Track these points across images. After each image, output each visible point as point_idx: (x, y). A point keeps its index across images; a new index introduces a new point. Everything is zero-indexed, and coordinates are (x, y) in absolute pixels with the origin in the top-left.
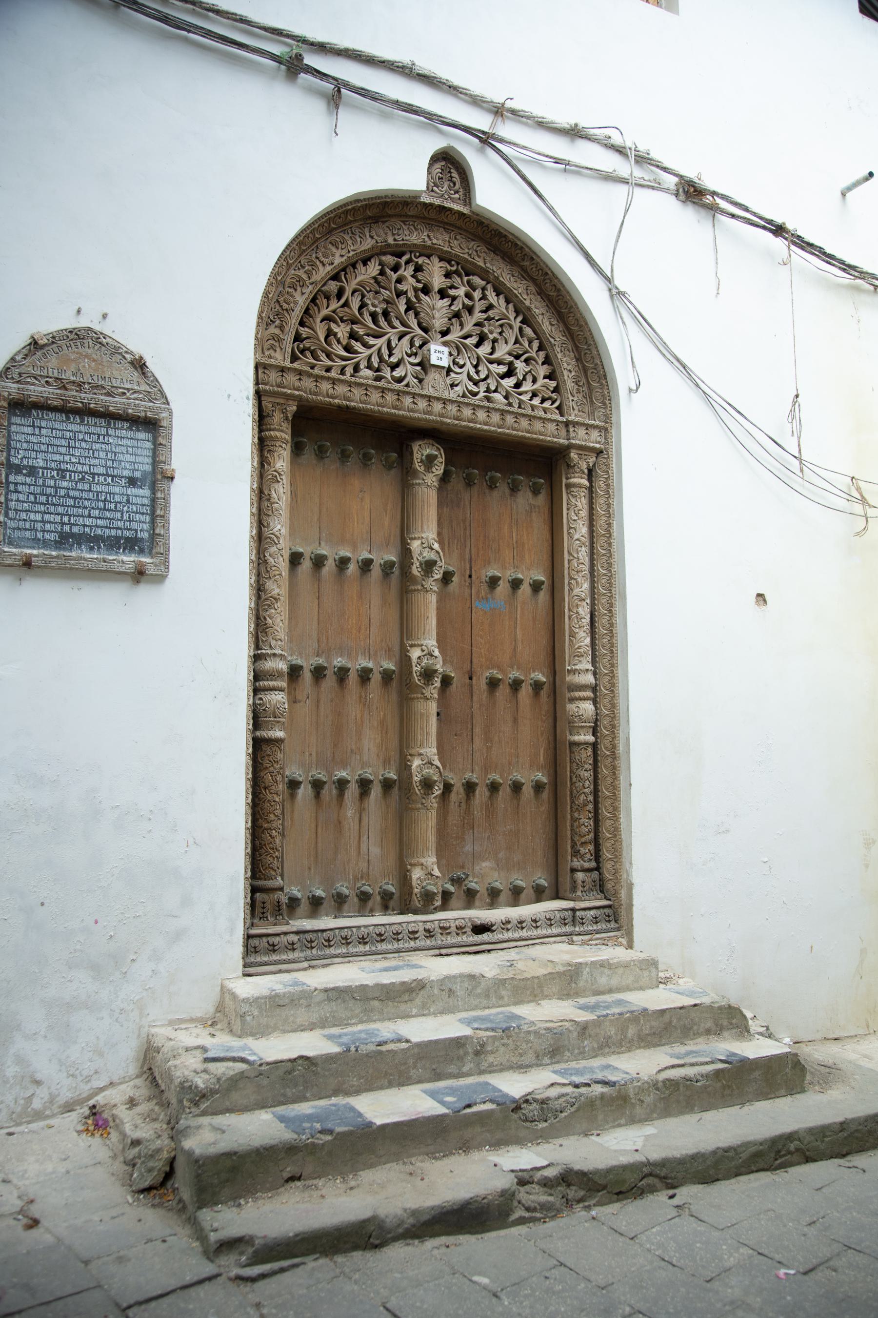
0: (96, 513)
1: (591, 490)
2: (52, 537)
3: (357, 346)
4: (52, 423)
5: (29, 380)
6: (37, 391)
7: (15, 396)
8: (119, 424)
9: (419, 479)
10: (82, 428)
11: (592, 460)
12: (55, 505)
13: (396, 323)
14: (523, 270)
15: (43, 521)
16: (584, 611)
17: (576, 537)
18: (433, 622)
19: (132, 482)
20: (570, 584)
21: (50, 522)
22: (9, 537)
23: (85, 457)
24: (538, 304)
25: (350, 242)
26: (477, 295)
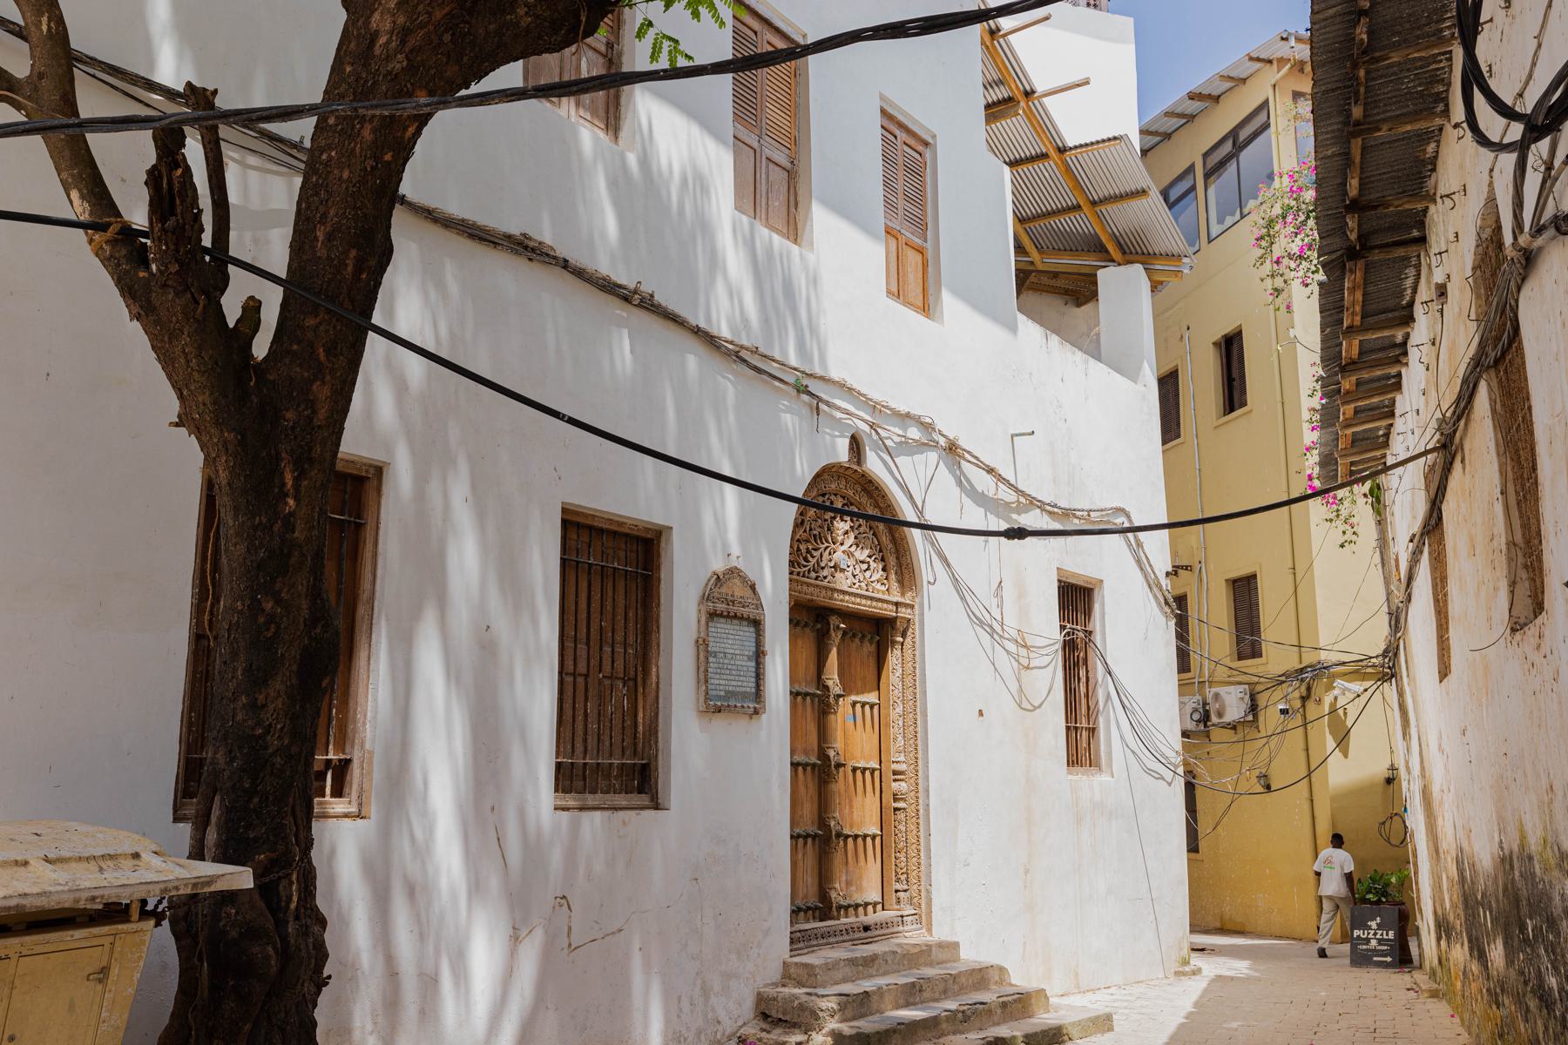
6: (721, 607)
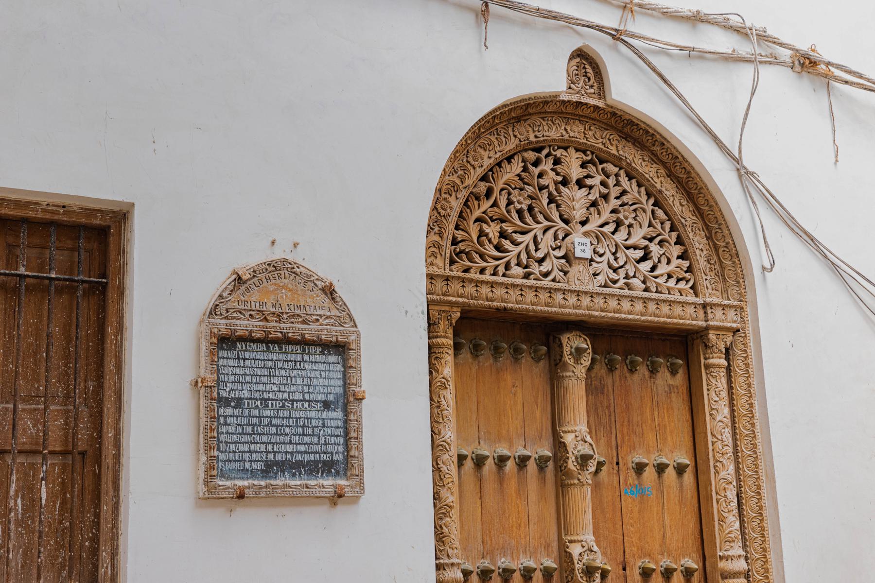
0: (296, 439)
1: (729, 369)
2: (258, 466)
3: (507, 244)
4: (253, 352)
5: (235, 315)
6: (243, 325)
7: (224, 332)
8: (313, 349)
9: (569, 371)
10: (281, 357)
11: (729, 340)
12: (260, 434)
13: (540, 218)
14: (653, 154)
15: (250, 452)
16: (732, 494)
17: (719, 418)
18: (589, 516)
19: (326, 405)
20: (715, 467)
21: (256, 452)
22: (221, 470)
23: (285, 385)
24: (669, 186)
25: (496, 143)
26: (611, 181)
